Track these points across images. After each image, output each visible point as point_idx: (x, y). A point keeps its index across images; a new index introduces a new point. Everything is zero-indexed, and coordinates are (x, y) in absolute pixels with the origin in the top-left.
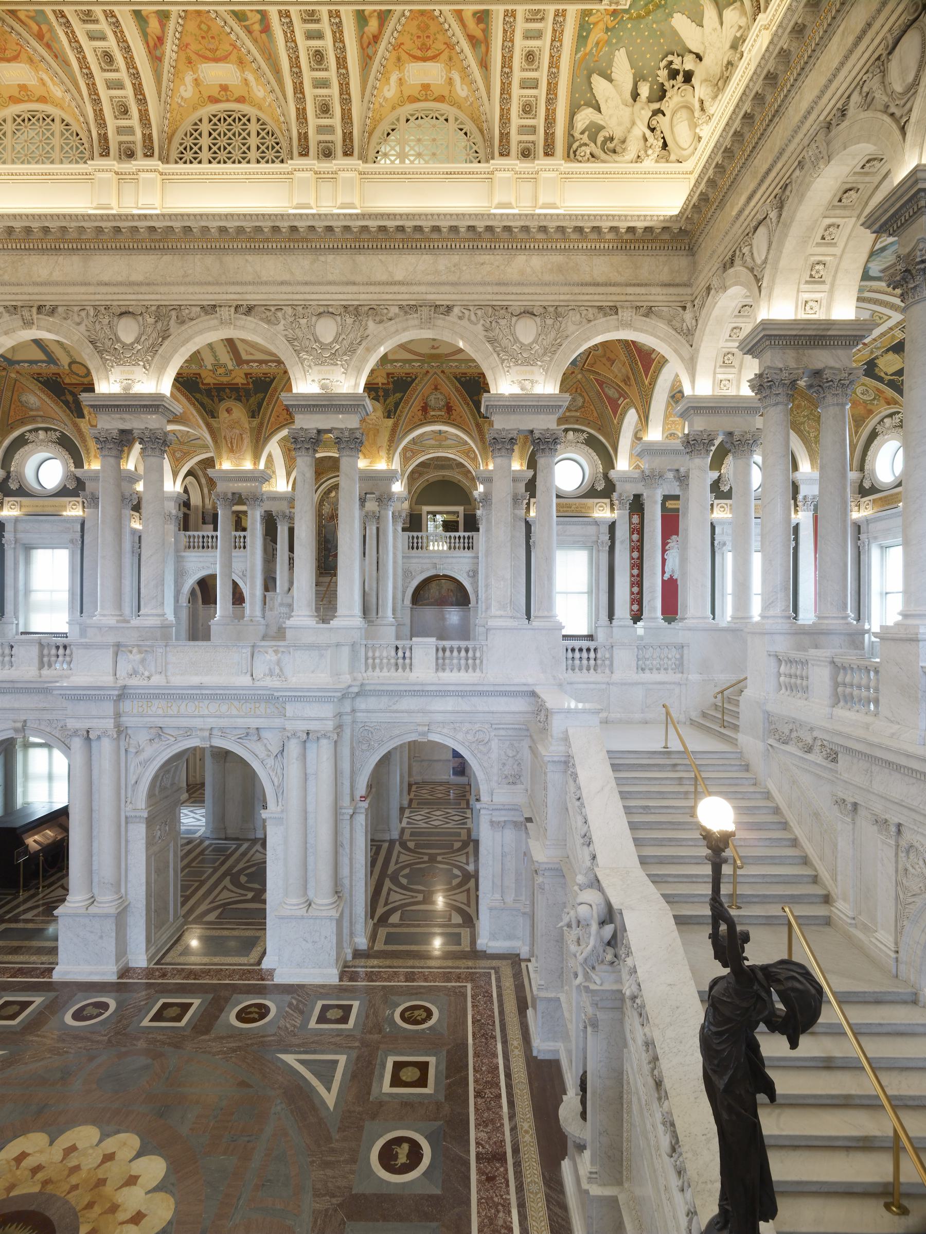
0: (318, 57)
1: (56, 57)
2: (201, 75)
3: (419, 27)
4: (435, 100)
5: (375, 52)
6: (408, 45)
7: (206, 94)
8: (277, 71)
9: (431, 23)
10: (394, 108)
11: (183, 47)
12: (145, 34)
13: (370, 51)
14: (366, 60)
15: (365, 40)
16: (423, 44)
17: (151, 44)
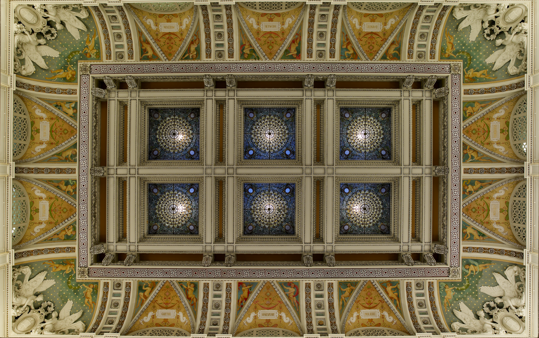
0: (220, 35)
1: (346, 35)
2: (280, 26)
3: (172, 48)
4: (164, 15)
5: (192, 37)
6: (177, 40)
7: (281, 18)
8: (241, 30)
9: (166, 50)
10: (184, 13)
11: (283, 39)
12: (300, 44)
13: (195, 37)
14: (197, 34)
15: (197, 42)
16: (170, 40)
17: (298, 40)
